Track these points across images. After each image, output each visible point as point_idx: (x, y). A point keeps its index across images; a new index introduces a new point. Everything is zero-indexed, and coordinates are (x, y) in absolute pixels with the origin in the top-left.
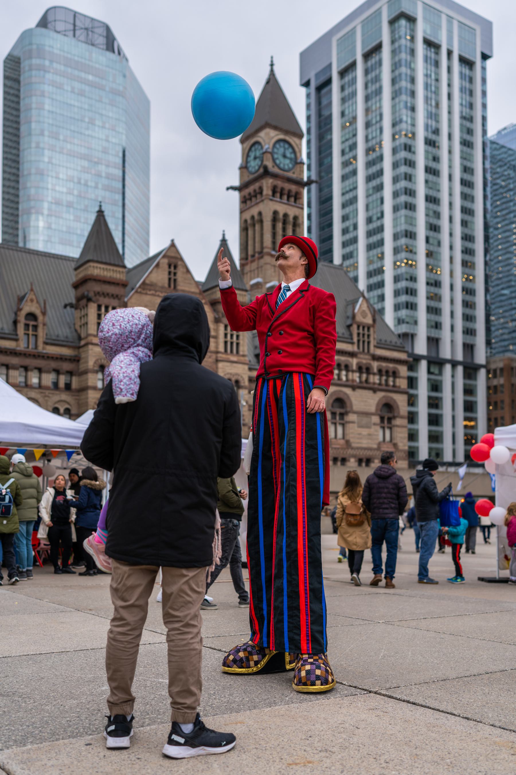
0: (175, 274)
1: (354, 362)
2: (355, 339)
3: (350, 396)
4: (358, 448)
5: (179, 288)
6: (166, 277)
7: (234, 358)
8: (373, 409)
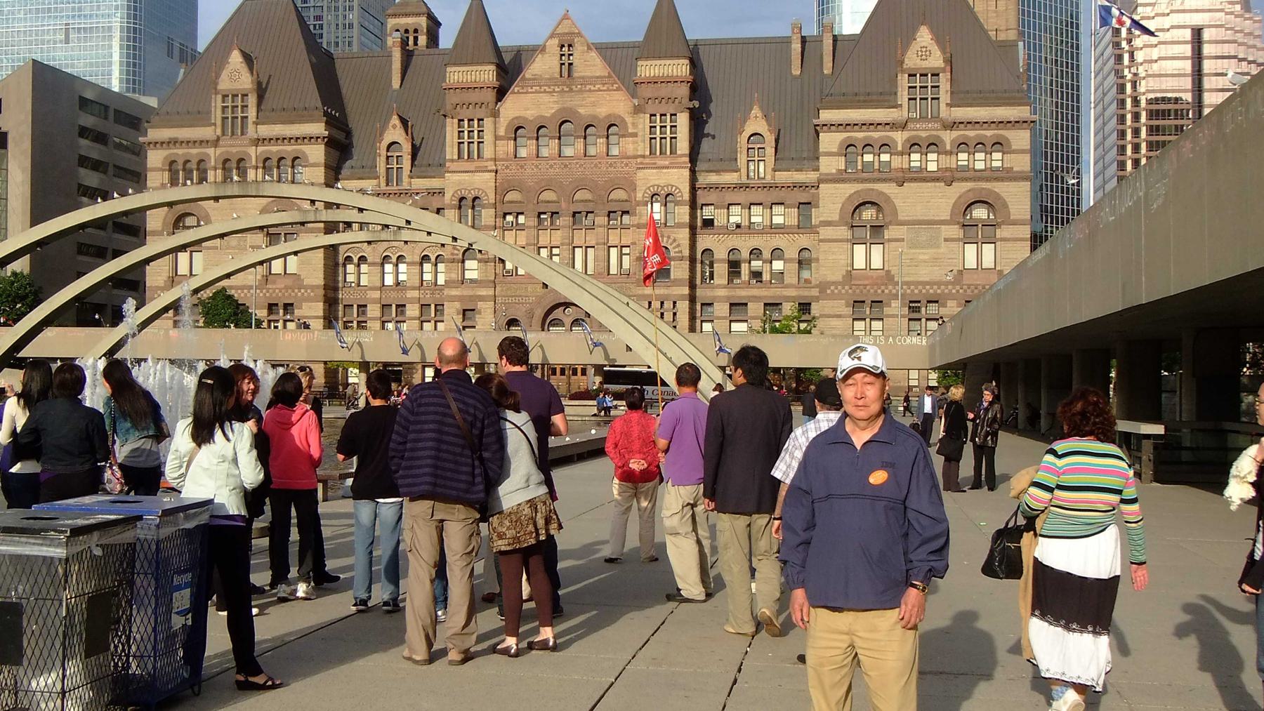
1: (899, 137)
2: (903, 96)
3: (892, 196)
5: (575, 75)
6: (556, 63)
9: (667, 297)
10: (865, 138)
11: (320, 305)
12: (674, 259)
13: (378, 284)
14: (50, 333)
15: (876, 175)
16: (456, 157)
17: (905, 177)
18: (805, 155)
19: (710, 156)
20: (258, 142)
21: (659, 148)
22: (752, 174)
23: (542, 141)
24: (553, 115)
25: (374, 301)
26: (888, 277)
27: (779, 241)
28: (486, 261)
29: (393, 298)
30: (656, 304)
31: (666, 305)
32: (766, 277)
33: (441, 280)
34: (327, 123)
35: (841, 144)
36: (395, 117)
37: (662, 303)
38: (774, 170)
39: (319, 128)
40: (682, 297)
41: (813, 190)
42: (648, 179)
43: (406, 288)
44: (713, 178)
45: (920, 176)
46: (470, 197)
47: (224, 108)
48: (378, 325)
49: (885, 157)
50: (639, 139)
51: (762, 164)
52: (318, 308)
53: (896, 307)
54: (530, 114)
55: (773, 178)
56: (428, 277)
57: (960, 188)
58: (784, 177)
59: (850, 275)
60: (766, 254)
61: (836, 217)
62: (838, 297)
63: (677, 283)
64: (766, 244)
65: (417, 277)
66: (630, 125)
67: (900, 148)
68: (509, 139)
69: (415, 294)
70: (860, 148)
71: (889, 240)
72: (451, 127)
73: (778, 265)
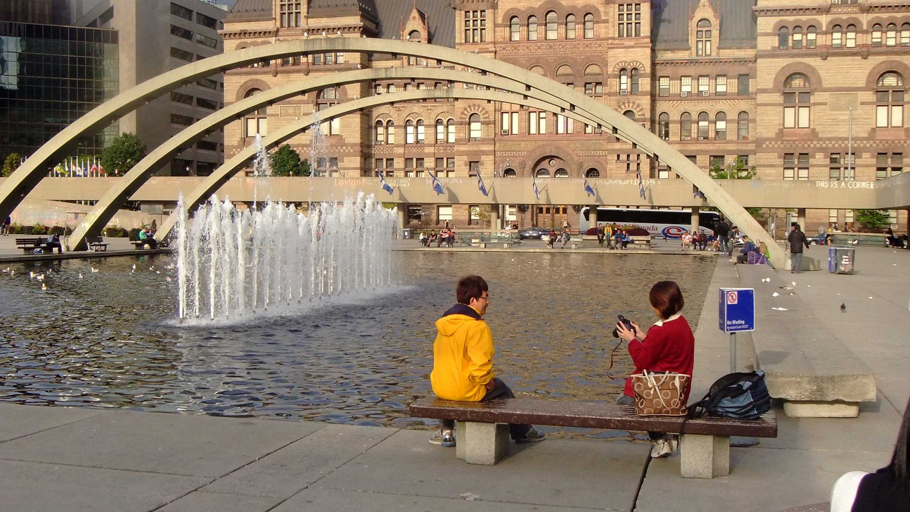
1: (824, 20)
4: (830, 139)
7: (632, 43)
8: (862, 83)
10: (797, 20)
11: (358, 159)
13: (403, 142)
14: (154, 181)
15: (804, 51)
16: (463, 41)
17: (828, 53)
18: (744, 35)
19: (666, 38)
21: (627, 31)
22: (700, 52)
23: (532, 27)
24: (540, 6)
25: (399, 156)
26: (814, 134)
27: (722, 106)
28: (488, 123)
29: (414, 153)
30: (623, 157)
31: (631, 158)
32: (712, 134)
33: (452, 139)
34: (362, 16)
35: (776, 25)
36: (415, 11)
37: (628, 156)
38: (719, 48)
39: (355, 20)
41: (751, 65)
42: (618, 57)
43: (424, 146)
44: (669, 56)
45: (841, 52)
47: (282, 5)
48: (402, 174)
49: (811, 36)
50: (610, 24)
51: (708, 43)
52: (356, 161)
53: (820, 158)
55: (718, 54)
56: (441, 136)
57: (875, 61)
58: (727, 54)
59: (782, 133)
60: (712, 117)
61: (770, 85)
62: (773, 150)
64: (712, 108)
65: (433, 136)
66: (602, 14)
67: (824, 29)
68: (505, 26)
69: (431, 150)
70: (791, 29)
71: (815, 104)
72: (460, 17)
73: (721, 125)
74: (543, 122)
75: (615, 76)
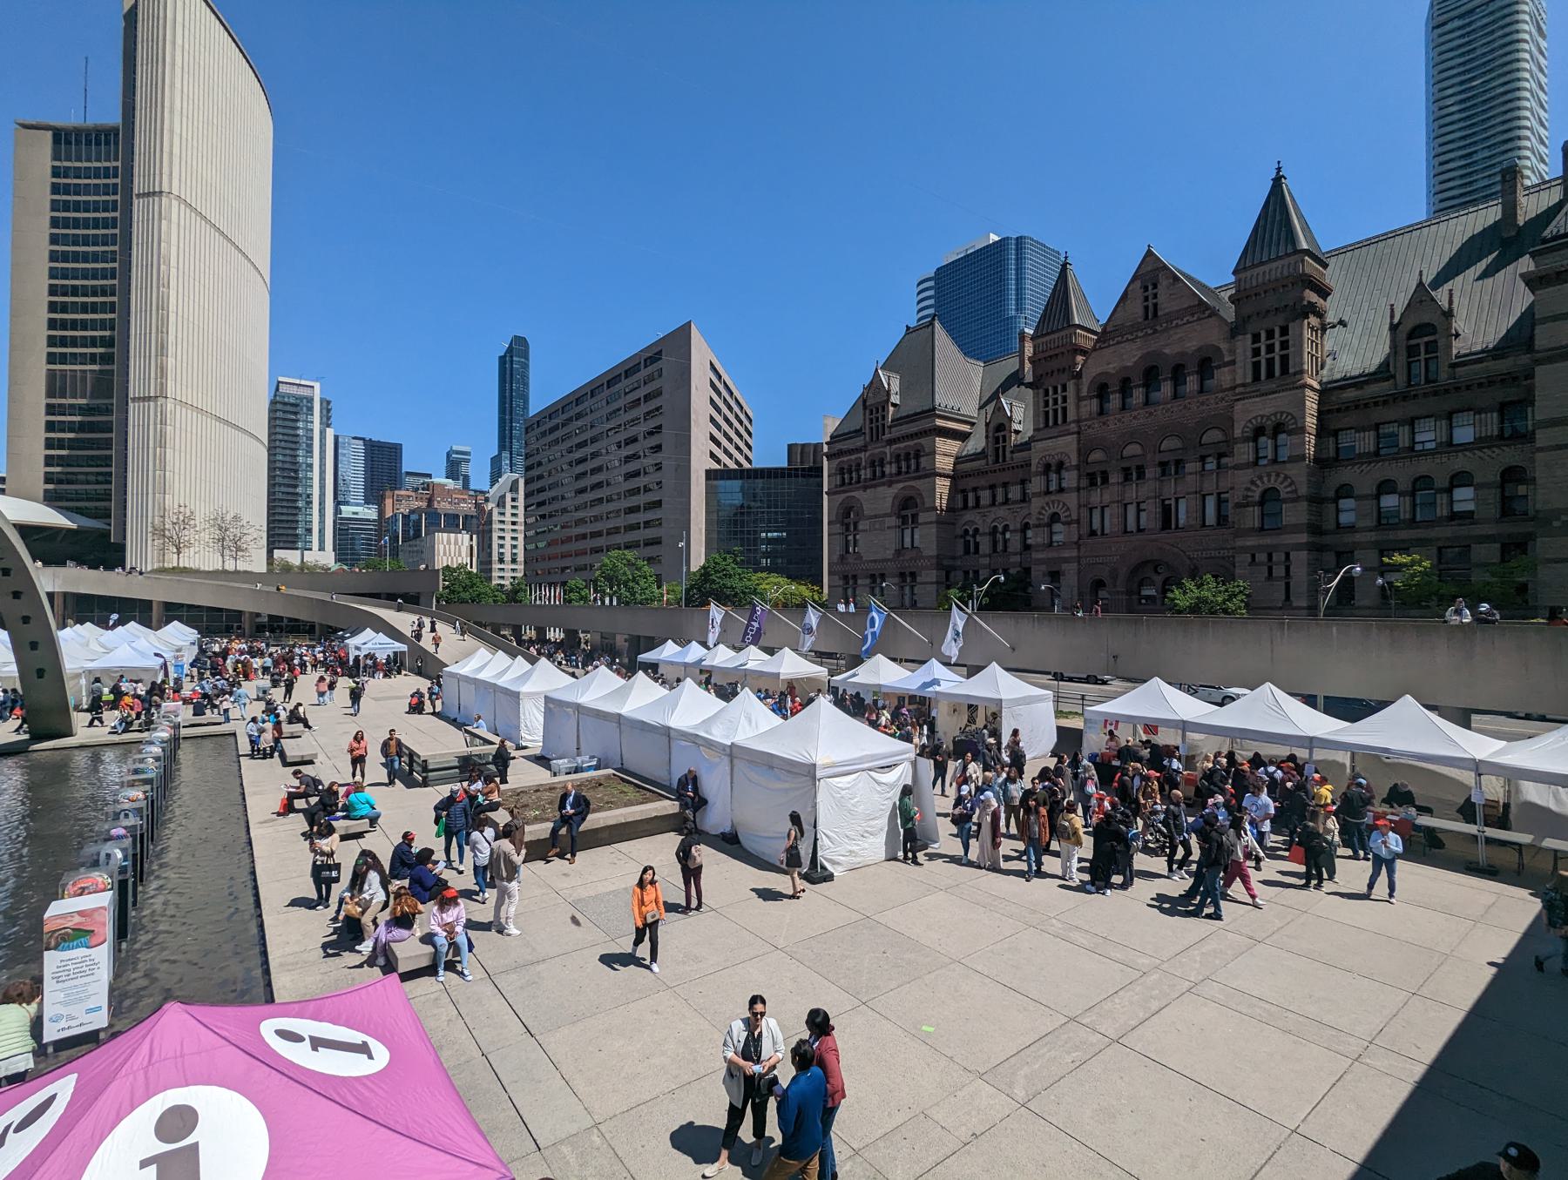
0: (1155, 296)
9: (1276, 547)
12: (1285, 501)
20: (891, 442)
40: (1298, 547)
46: (1053, 462)
54: (1112, 368)
63: (1295, 529)
74: (1143, 515)
75: (1246, 440)
